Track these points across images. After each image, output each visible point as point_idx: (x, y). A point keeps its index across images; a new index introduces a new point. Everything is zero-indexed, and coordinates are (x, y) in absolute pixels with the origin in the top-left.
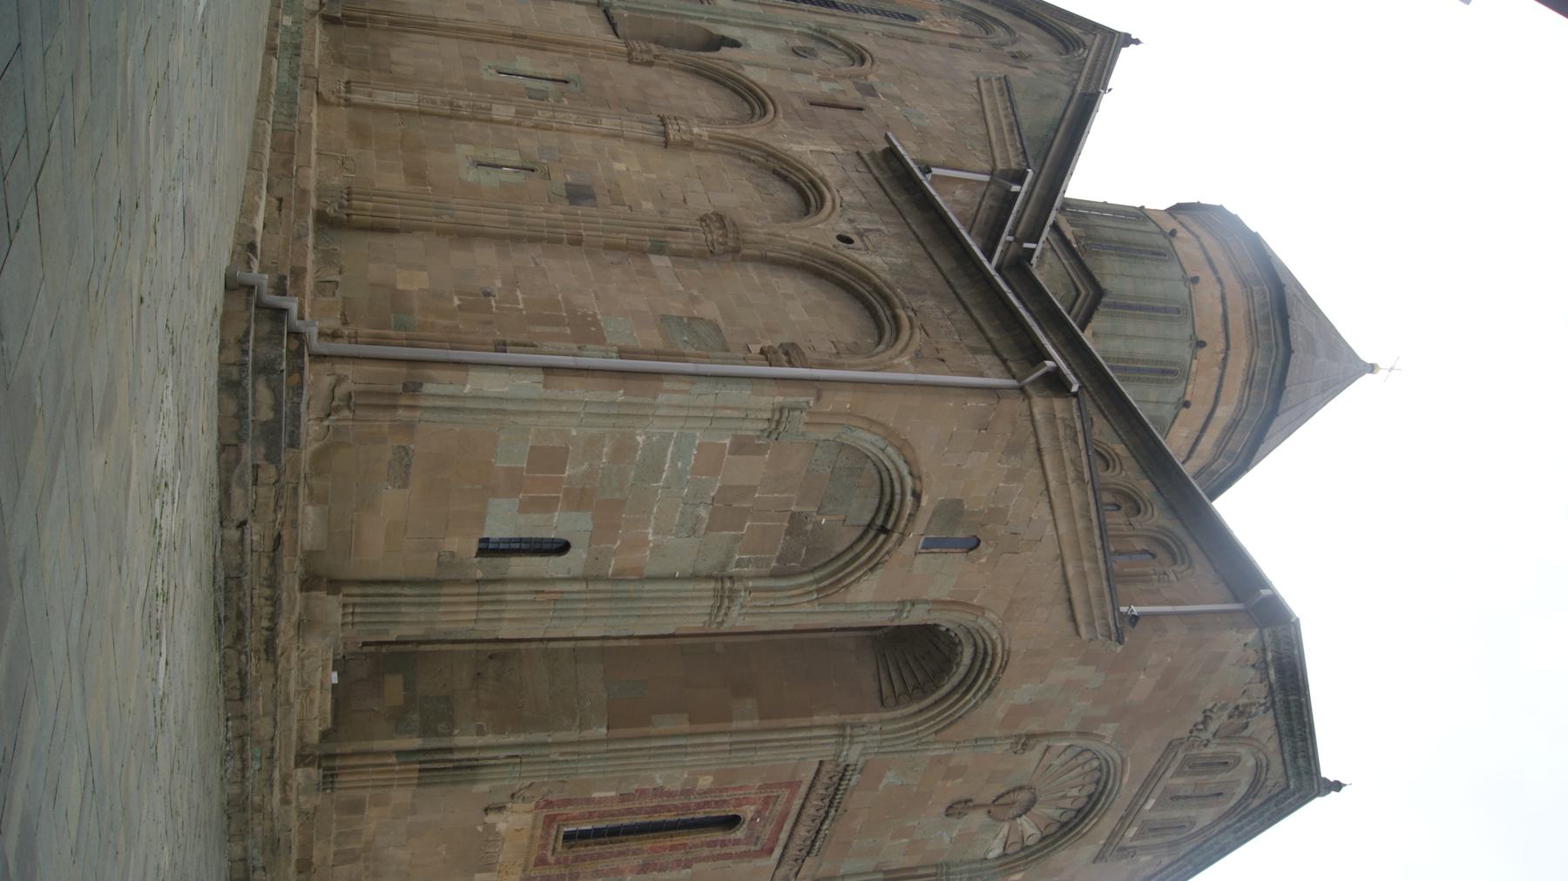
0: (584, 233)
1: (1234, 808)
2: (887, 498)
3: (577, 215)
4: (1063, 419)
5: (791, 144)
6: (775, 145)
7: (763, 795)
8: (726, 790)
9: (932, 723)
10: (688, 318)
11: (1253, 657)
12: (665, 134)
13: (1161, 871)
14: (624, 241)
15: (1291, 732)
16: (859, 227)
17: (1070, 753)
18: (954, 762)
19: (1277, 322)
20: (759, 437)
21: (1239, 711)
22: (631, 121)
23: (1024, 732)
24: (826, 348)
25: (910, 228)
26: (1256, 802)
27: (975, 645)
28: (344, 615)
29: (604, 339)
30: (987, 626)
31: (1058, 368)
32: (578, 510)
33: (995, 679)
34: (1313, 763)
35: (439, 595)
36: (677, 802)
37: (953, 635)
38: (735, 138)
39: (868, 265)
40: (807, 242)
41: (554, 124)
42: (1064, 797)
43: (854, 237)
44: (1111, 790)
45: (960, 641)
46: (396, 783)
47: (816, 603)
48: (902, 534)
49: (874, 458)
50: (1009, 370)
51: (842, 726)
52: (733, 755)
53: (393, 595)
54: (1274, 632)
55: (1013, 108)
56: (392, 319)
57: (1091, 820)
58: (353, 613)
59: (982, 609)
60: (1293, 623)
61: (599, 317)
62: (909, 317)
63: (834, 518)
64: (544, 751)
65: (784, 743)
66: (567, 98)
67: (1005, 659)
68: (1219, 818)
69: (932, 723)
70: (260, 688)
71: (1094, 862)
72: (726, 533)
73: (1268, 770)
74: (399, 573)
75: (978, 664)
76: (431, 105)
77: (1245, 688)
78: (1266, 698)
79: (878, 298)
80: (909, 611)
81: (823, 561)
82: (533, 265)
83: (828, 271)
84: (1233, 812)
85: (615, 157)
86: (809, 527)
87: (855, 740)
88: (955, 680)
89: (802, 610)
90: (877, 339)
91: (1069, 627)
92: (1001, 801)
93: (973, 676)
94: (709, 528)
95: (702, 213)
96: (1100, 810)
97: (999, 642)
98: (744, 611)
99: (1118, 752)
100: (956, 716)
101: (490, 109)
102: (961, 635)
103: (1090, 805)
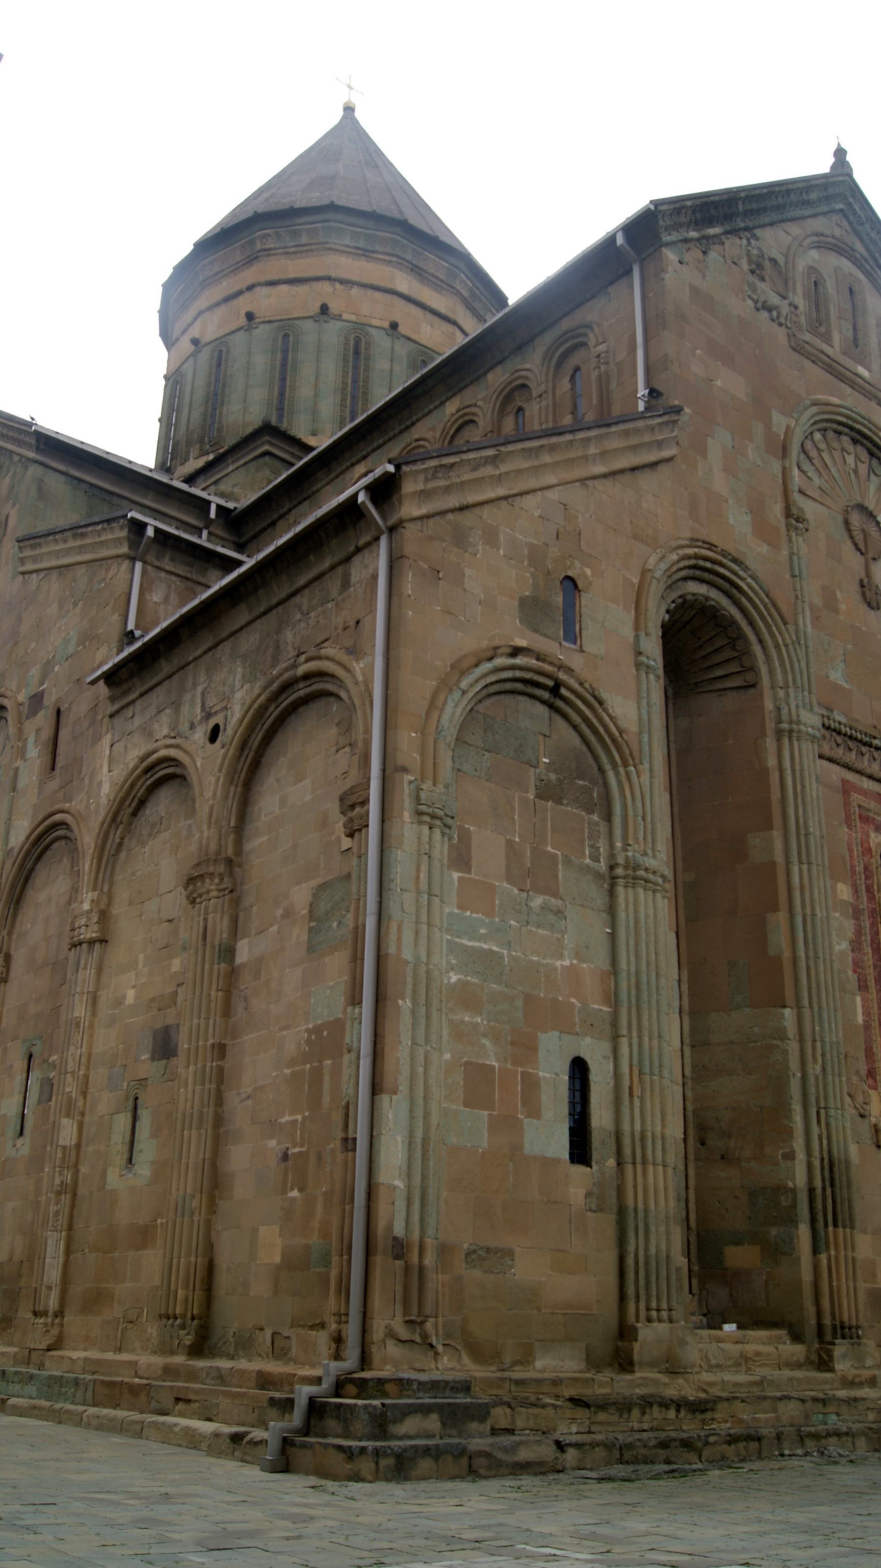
0: (211, 1041)
1: (867, 274)
3: (189, 1049)
4: (426, 480)
5: (102, 794)
6: (103, 814)
7: (858, 824)
9: (774, 628)
10: (310, 920)
11: (696, 254)
12: (91, 942)
14: (220, 994)
16: (199, 718)
17: (806, 466)
18: (818, 602)
20: (450, 839)
21: (757, 269)
22: (76, 983)
23: (783, 520)
24: (343, 759)
25: (200, 657)
26: (859, 247)
27: (685, 579)
28: (660, 1320)
29: (337, 1020)
31: (368, 488)
33: (724, 556)
35: (636, 1210)
37: (673, 605)
38: (95, 861)
39: (246, 707)
40: (218, 779)
41: (82, 1072)
42: (856, 471)
43: (212, 723)
45: (680, 597)
46: (850, 1254)
47: (640, 767)
48: (560, 668)
49: (473, 703)
50: (368, 545)
51: (779, 733)
52: (814, 861)
53: (637, 1263)
55: (55, 533)
56: (317, 1270)
58: (658, 1310)
59: (644, 573)
60: (656, 206)
61: (311, 1026)
62: (307, 660)
63: (542, 748)
64: (812, 1080)
65: (800, 801)
66: (50, 1055)
67: (700, 544)
69: (774, 628)
70: (745, 1417)
72: (560, 875)
73: (822, 235)
74: (610, 1257)
76: (60, 1217)
77: (729, 262)
78: (741, 238)
79: (284, 696)
80: (648, 657)
81: (591, 761)
83: (252, 754)
84: (871, 275)
85: (120, 1001)
87: (794, 718)
88: (725, 602)
89: (648, 783)
90: (332, 699)
91: (664, 469)
92: (861, 546)
93: (720, 582)
95: (185, 902)
96: (870, 430)
98: (649, 852)
99: (806, 409)
100: (767, 600)
101: (64, 1148)
102: (674, 595)
103: (865, 442)
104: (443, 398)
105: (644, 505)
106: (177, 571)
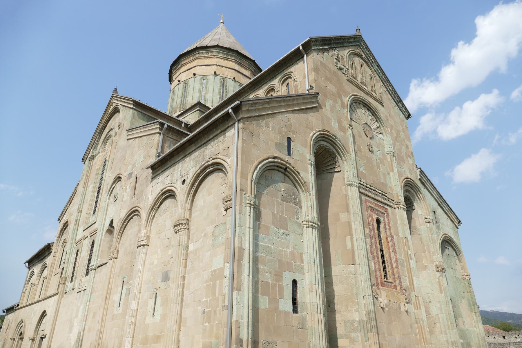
0: (180, 275)
2: (276, 168)
4: (249, 107)
5: (149, 201)
8: (369, 223)
10: (213, 237)
12: (144, 245)
13: (385, 85)
15: (343, 43)
16: (179, 178)
19: (208, 49)
22: (139, 258)
24: (223, 188)
27: (320, 140)
29: (221, 268)
30: (315, 136)
31: (232, 108)
32: (282, 277)
34: (352, 37)
36: (373, 240)
37: (317, 147)
38: (146, 221)
40: (185, 195)
41: (139, 286)
43: (183, 179)
44: (362, 99)
45: (319, 145)
50: (231, 125)
54: (313, 46)
57: (371, 106)
60: (311, 39)
61: (212, 270)
66: (129, 281)
68: (369, 67)
71: (383, 106)
75: (326, 140)
76: (130, 333)
78: (333, 50)
79: (205, 170)
82: (192, 295)
83: (195, 188)
85: (152, 264)
86: (285, 195)
88: (331, 147)
94: (287, 230)
95: (174, 232)
97: (320, 132)
100: (343, 147)
101: (133, 310)
102: (318, 145)
104: (250, 93)
105: (309, 119)
106: (173, 138)
